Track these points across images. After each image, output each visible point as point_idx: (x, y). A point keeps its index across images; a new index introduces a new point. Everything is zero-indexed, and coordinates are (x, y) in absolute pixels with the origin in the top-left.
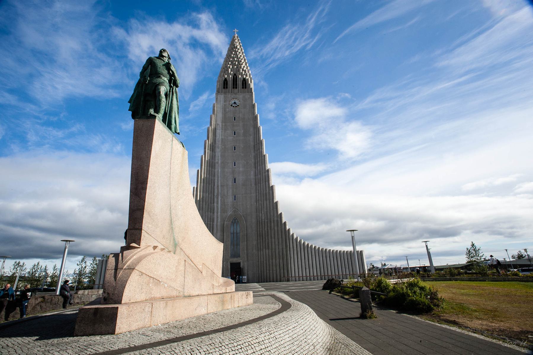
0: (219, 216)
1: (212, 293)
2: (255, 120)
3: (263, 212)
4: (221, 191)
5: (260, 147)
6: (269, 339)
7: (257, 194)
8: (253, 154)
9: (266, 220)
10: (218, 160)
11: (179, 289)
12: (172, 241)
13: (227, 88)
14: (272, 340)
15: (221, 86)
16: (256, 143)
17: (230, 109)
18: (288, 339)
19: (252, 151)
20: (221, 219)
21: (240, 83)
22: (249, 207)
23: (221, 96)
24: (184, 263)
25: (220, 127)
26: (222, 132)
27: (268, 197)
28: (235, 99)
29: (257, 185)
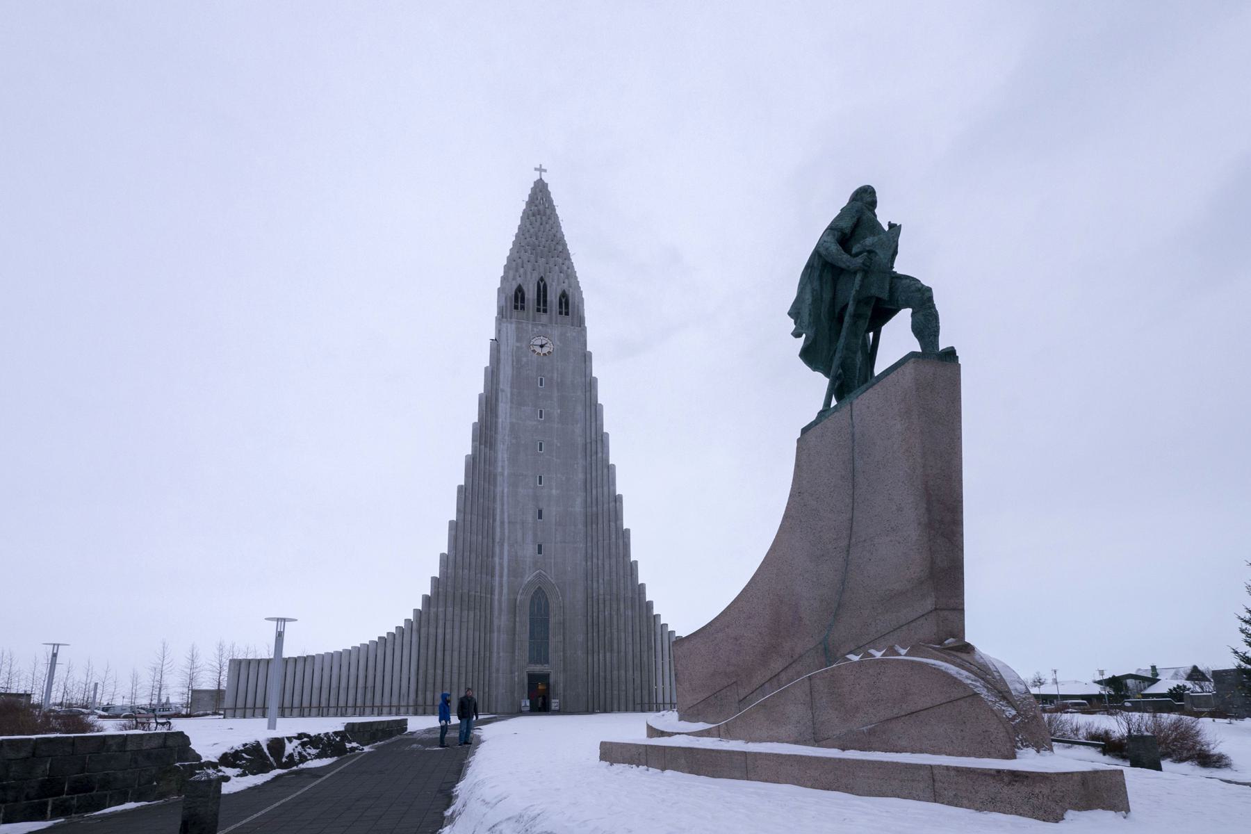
0: (504, 582)
2: (588, 389)
3: (601, 581)
4: (509, 532)
5: (599, 450)
7: (589, 544)
8: (581, 462)
9: (608, 597)
10: (503, 467)
13: (523, 308)
15: (509, 304)
16: (588, 441)
17: (530, 358)
19: (579, 456)
20: (508, 588)
22: (569, 569)
23: (509, 325)
25: (507, 397)
26: (511, 408)
27: (613, 551)
28: (542, 337)
29: (589, 528)
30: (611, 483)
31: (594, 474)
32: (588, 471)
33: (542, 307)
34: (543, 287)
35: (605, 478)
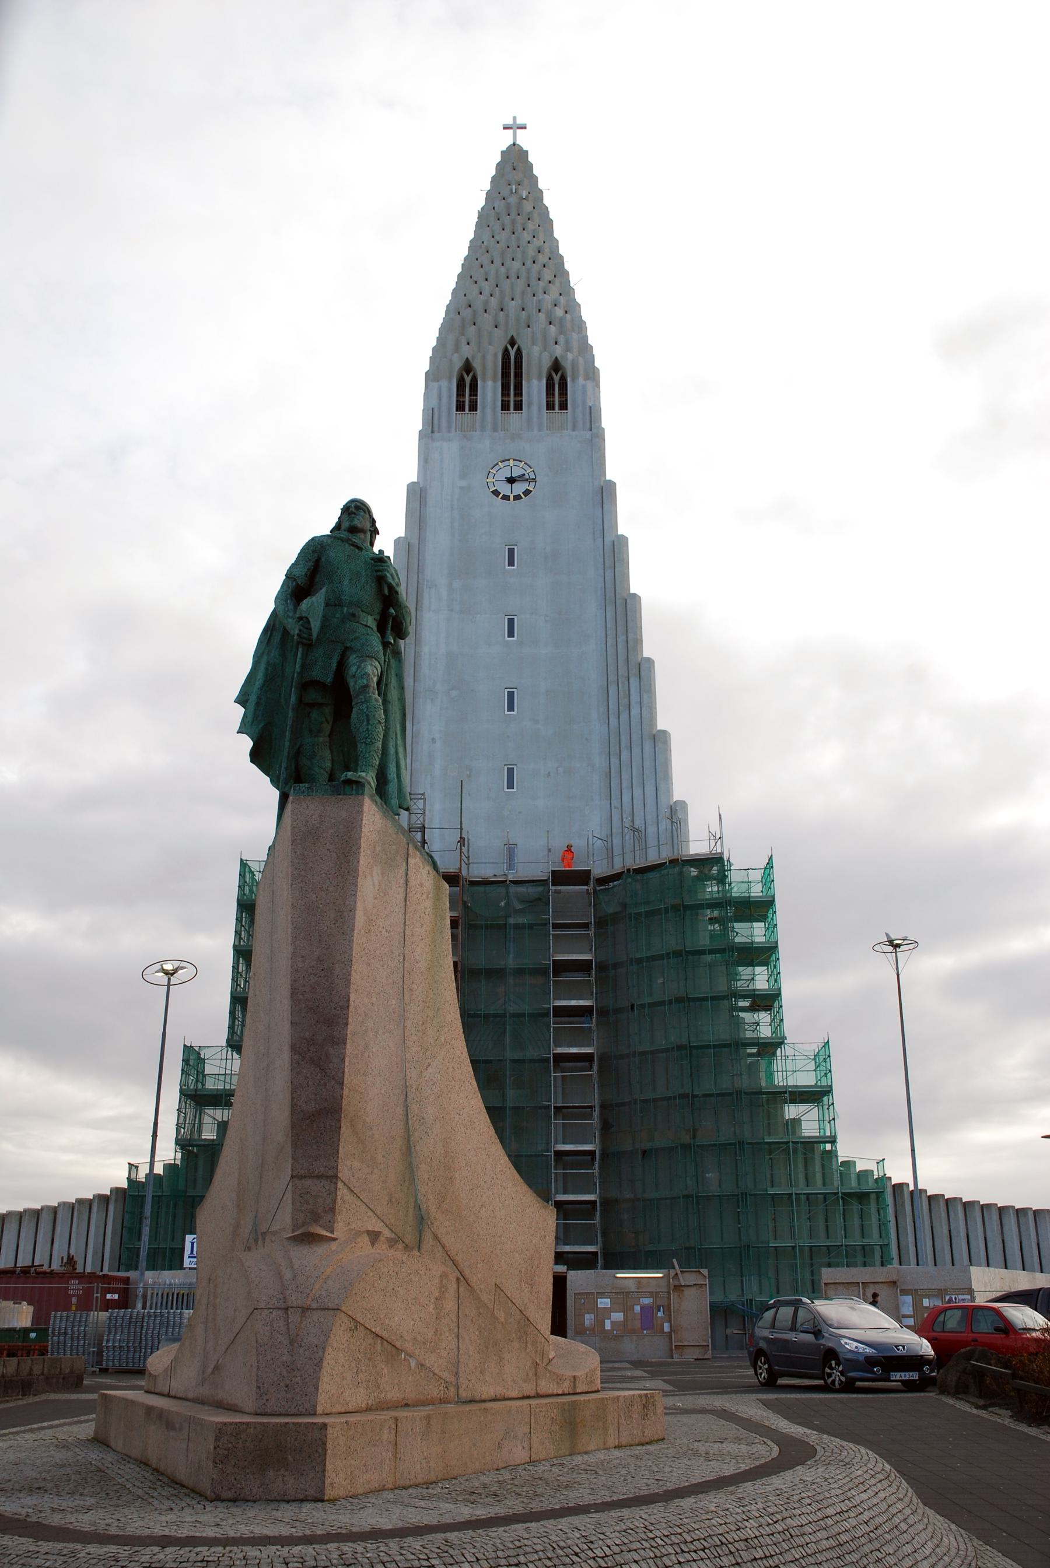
1: (532, 1393)
2: (609, 563)
6: (772, 1534)
11: (445, 1375)
12: (411, 1210)
14: (781, 1540)
15: (445, 400)
18: (825, 1544)
21: (535, 389)
24: (455, 1286)
30: (660, 775)
31: (625, 754)
32: (614, 749)
33: (512, 398)
34: (516, 358)
35: (648, 764)
